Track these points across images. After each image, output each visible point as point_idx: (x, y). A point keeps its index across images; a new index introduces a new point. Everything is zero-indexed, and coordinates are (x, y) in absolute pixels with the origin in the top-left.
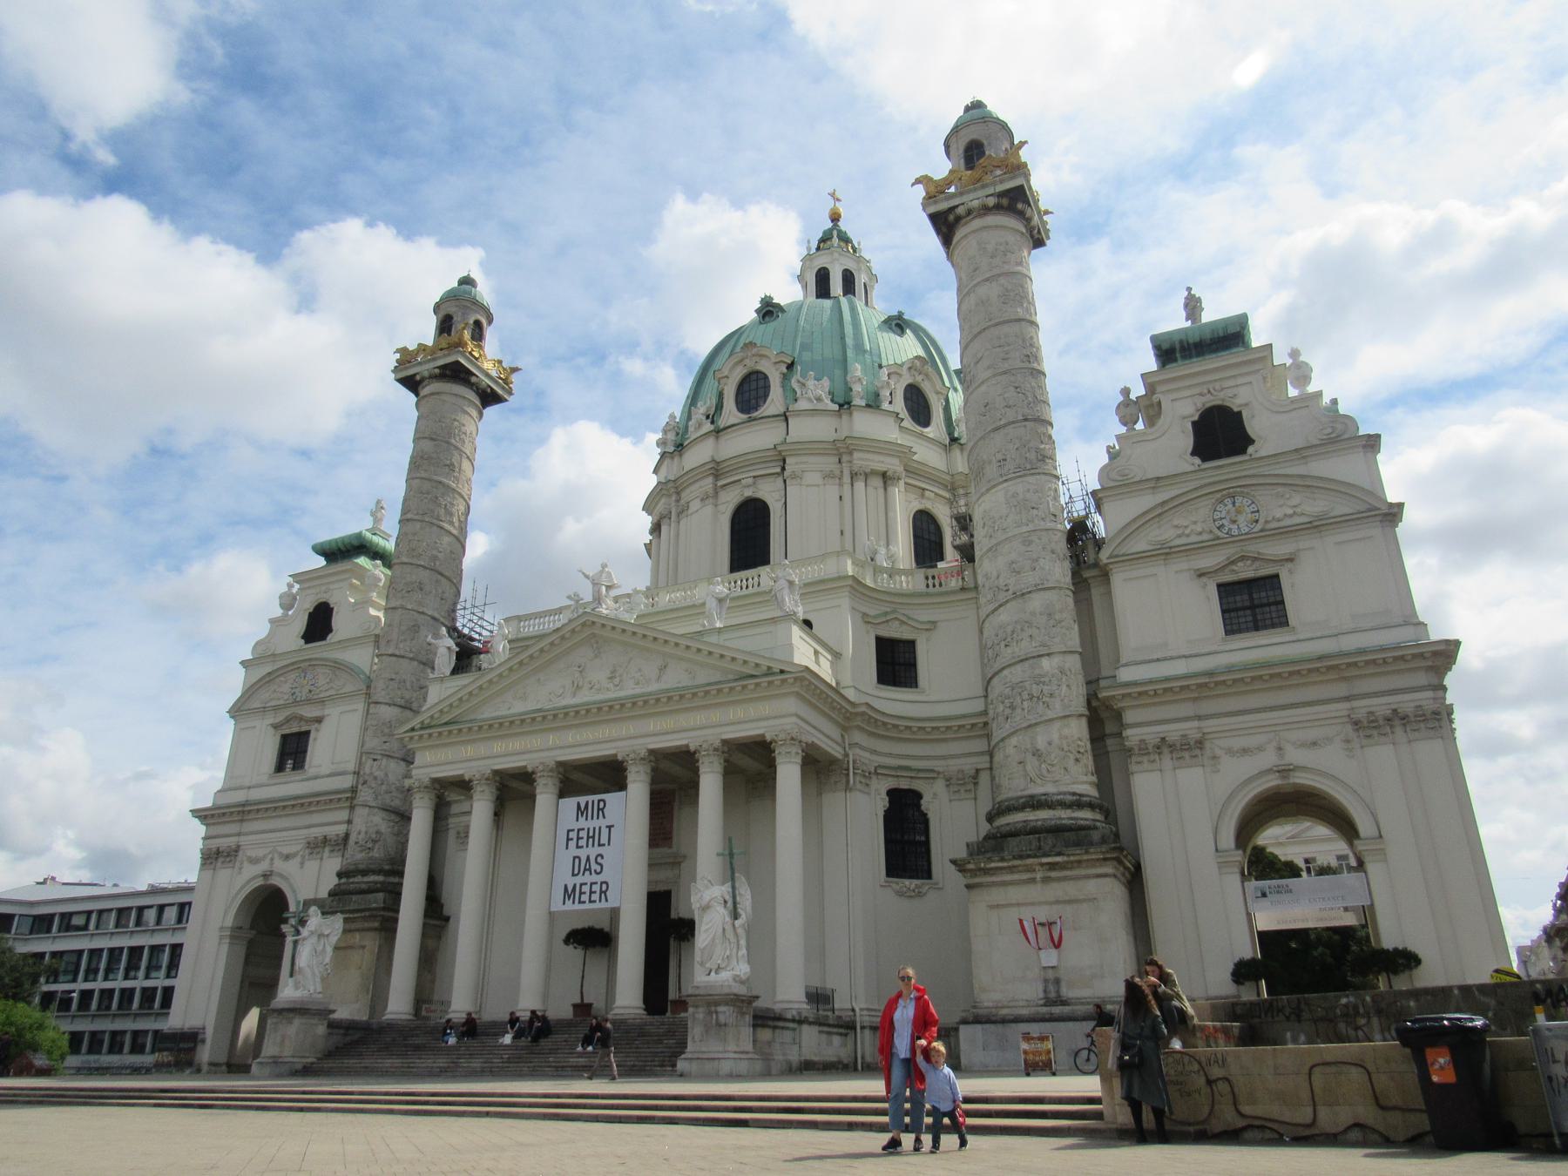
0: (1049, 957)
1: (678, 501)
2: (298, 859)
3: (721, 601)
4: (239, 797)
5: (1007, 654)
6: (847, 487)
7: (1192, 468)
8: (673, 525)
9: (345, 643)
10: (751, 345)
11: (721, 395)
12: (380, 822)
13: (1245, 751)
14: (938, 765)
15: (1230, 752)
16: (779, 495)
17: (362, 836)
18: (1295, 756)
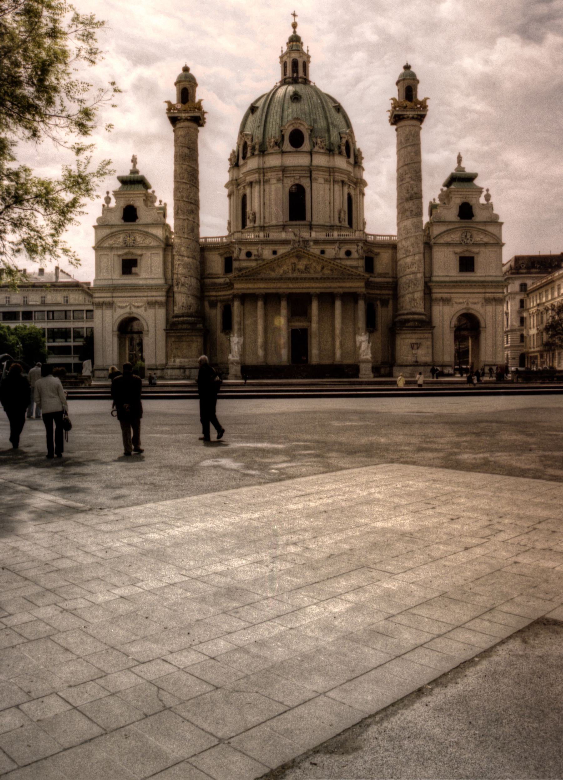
0: (414, 352)
1: (264, 176)
2: (143, 309)
3: (340, 249)
4: (110, 282)
5: (408, 271)
6: (332, 186)
7: (456, 220)
8: (262, 187)
9: (147, 225)
10: (297, 119)
11: (283, 137)
12: (191, 300)
13: (460, 303)
14: (379, 297)
15: (456, 303)
16: (309, 184)
17: (185, 305)
18: (471, 306)
